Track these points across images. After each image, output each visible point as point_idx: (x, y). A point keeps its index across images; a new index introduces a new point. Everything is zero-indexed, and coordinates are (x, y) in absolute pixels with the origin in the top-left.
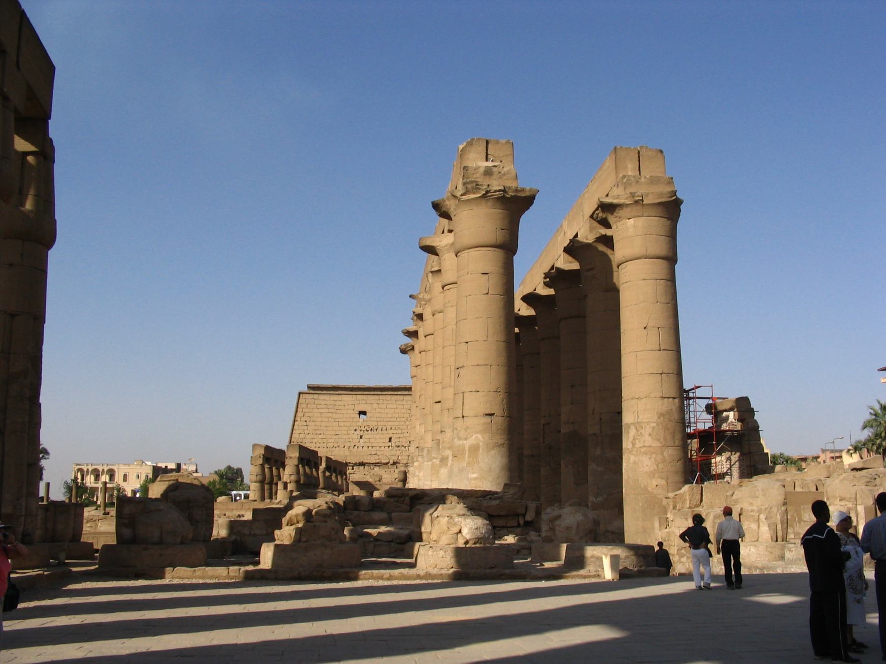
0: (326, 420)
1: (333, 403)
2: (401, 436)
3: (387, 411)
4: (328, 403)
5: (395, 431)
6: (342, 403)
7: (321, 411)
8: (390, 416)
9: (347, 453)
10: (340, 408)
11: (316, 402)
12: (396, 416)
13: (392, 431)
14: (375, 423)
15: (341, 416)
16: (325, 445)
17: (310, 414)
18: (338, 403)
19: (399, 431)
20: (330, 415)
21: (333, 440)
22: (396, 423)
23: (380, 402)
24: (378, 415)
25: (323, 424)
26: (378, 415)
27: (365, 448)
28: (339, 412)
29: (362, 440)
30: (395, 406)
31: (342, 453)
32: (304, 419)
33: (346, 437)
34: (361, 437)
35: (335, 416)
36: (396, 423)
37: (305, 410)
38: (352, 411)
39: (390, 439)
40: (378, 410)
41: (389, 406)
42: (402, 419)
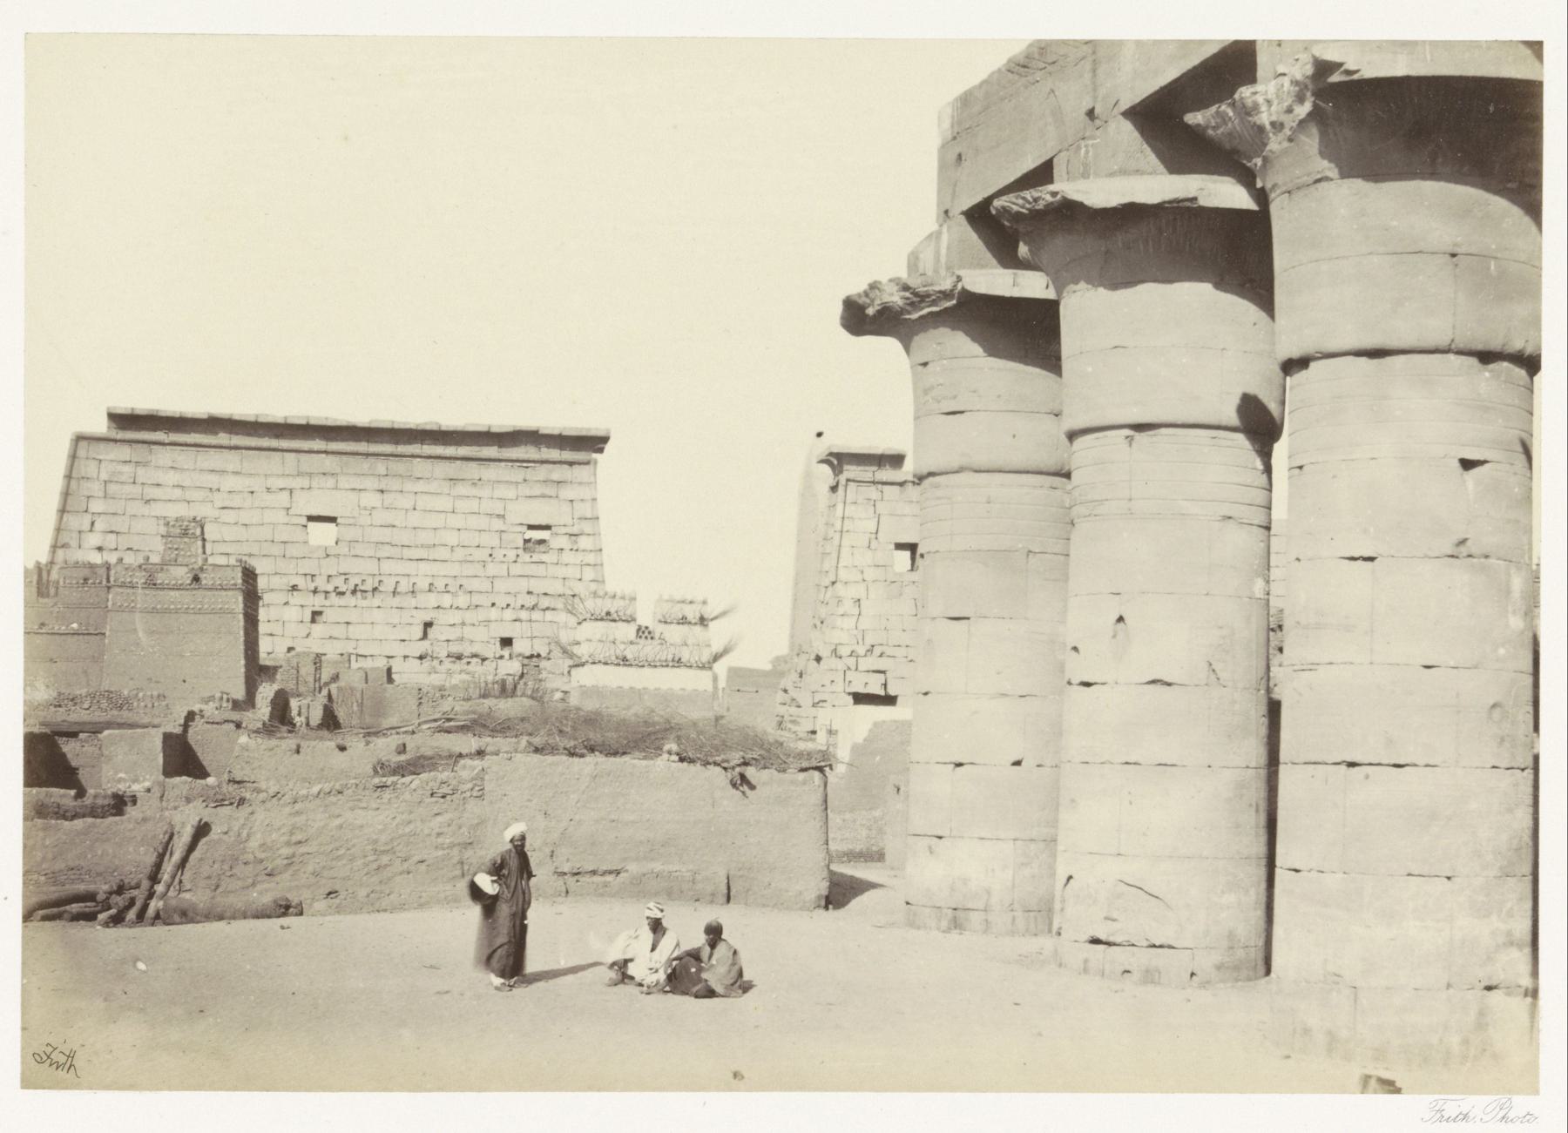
2: (470, 616)
3: (415, 519)
5: (447, 600)
8: (424, 537)
10: (236, 501)
13: (432, 600)
14: (371, 567)
17: (119, 524)
18: (230, 482)
19: (463, 600)
26: (385, 534)
28: (230, 516)
29: (318, 629)
34: (316, 615)
36: (454, 569)
38: (281, 517)
40: (381, 517)
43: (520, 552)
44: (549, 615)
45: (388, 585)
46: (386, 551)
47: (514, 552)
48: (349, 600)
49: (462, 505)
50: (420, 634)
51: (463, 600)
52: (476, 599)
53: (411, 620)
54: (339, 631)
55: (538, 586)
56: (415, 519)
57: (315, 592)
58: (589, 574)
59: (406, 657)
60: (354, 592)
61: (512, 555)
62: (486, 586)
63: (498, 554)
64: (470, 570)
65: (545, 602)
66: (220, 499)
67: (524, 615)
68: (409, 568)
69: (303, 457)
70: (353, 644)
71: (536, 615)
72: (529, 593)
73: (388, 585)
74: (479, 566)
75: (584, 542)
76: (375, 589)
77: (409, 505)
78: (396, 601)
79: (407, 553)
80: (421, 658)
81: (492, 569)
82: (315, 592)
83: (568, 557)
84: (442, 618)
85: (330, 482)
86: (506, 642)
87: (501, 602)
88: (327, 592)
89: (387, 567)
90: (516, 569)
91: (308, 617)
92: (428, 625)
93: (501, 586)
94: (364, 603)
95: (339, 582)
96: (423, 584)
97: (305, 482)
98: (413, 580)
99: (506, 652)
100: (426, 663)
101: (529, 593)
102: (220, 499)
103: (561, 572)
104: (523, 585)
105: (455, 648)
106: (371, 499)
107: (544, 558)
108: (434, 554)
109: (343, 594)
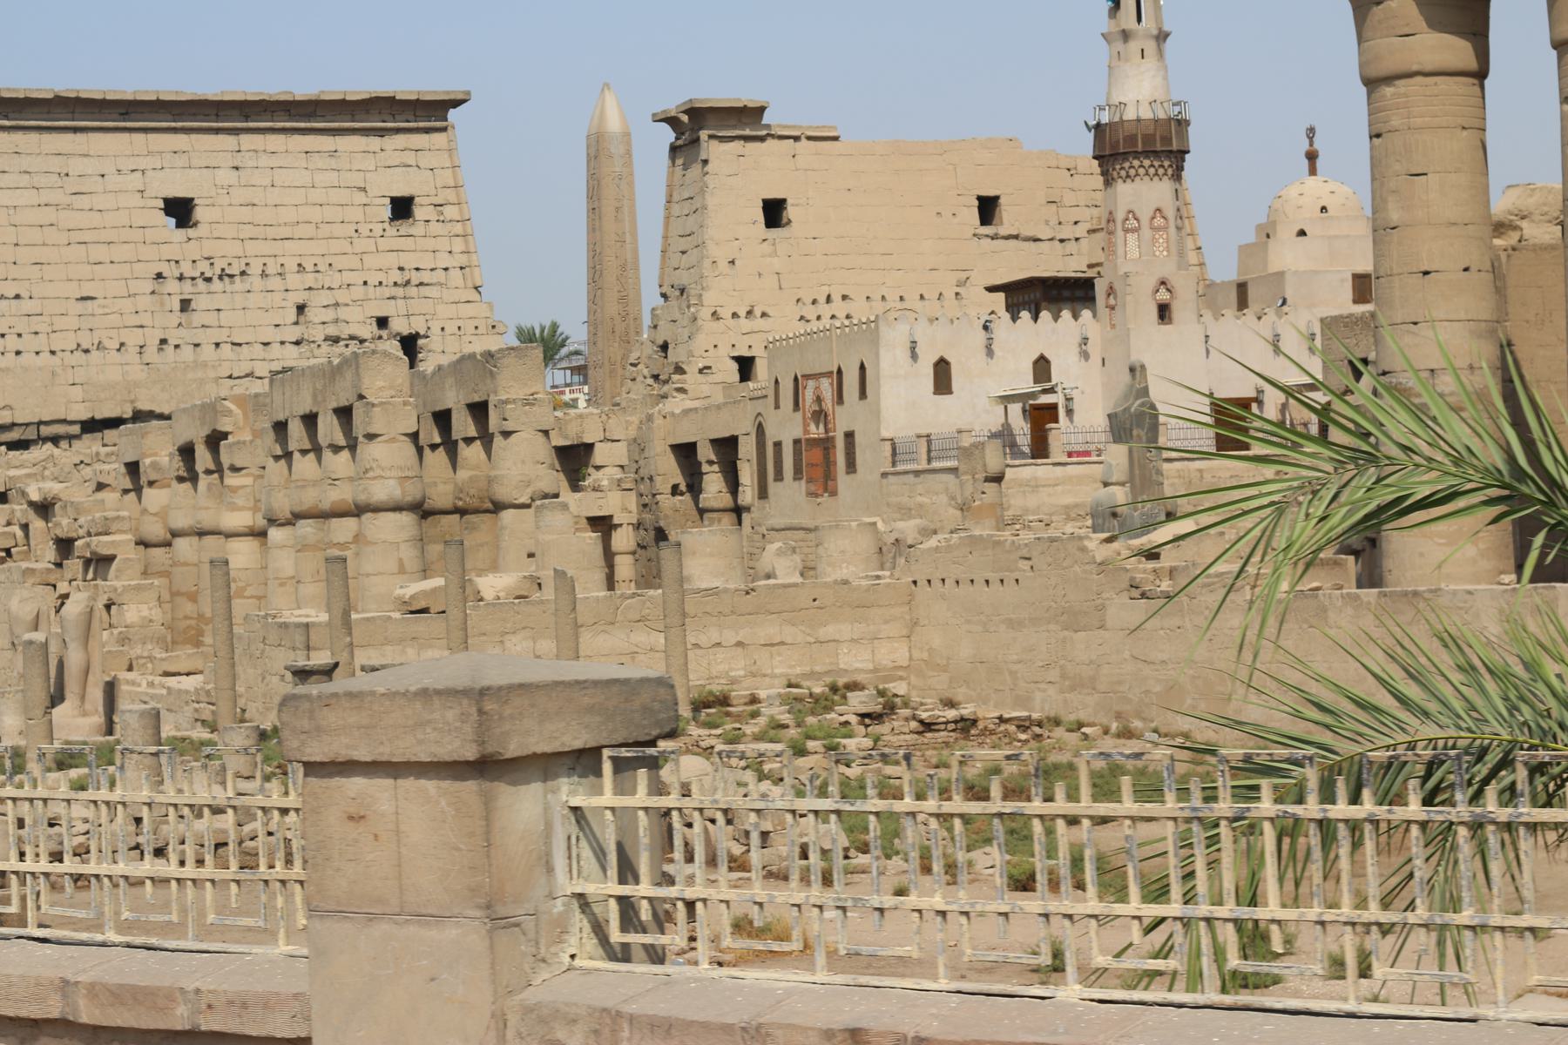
0: (35, 235)
3: (274, 196)
6: (90, 166)
8: (289, 215)
9: (137, 373)
12: (315, 214)
14: (236, 248)
16: (41, 342)
18: (76, 166)
20: (48, 215)
21: (73, 322)
22: (317, 247)
23: (247, 160)
25: (24, 254)
27: (208, 352)
28: (83, 202)
30: (303, 178)
31: (114, 374)
33: (127, 305)
34: (185, 305)
35: (67, 219)
36: (317, 247)
38: (136, 200)
39: (301, 309)
40: (240, 195)
41: (281, 177)
42: (338, 230)
43: (386, 225)
44: (424, 291)
45: (255, 269)
46: (248, 231)
48: (217, 285)
49: (320, 178)
50: (293, 318)
51: (335, 280)
52: (348, 277)
53: (284, 304)
54: (210, 319)
55: (409, 261)
56: (274, 196)
57: (181, 278)
58: (458, 245)
59: (282, 343)
60: (220, 278)
61: (378, 229)
62: (356, 264)
63: (364, 230)
64: (336, 246)
65: (416, 278)
67: (400, 292)
68: (277, 247)
69: (152, 136)
70: (225, 332)
71: (412, 291)
72: (401, 269)
74: (346, 243)
75: (451, 212)
76: (243, 273)
77: (268, 182)
79: (271, 232)
80: (297, 343)
81: (362, 244)
82: (181, 278)
83: (435, 228)
84: (318, 300)
85: (180, 161)
86: (382, 322)
87: (373, 281)
88: (193, 279)
89: (252, 248)
91: (177, 306)
92: (301, 309)
93: (370, 261)
94: (229, 288)
95: (203, 266)
96: (291, 265)
99: (384, 333)
100: (304, 348)
101: (401, 269)
102: (72, 185)
103: (430, 244)
104: (393, 260)
105: (332, 330)
106: (225, 176)
107: (412, 231)
109: (208, 280)
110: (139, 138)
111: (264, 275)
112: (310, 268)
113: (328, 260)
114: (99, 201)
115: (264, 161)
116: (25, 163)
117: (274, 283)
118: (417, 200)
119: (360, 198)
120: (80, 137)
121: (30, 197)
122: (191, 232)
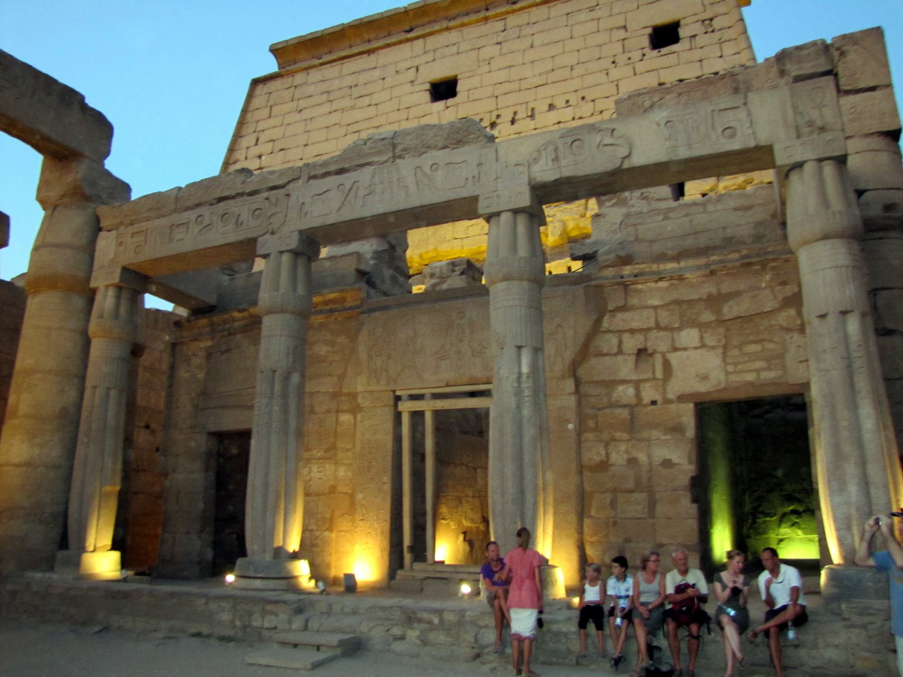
1: (350, 80)
3: (530, 55)
4: (336, 84)
6: (377, 74)
7: (306, 114)
10: (370, 88)
11: (298, 93)
12: (572, 59)
14: (490, 104)
15: (371, 111)
17: (275, 133)
18: (363, 78)
20: (336, 118)
24: (503, 75)
26: (503, 75)
28: (366, 101)
32: (255, 151)
35: (349, 117)
37: (261, 126)
38: (408, 88)
43: (647, 51)
47: (640, 53)
52: (600, 105)
61: (637, 55)
64: (590, 80)
66: (356, 92)
73: (507, 115)
77: (526, 43)
78: (517, 127)
79: (524, 85)
81: (615, 73)
85: (454, 49)
90: (640, 67)
96: (541, 107)
97: (429, 57)
98: (531, 106)
108: (552, 77)
110: (420, 42)
111: (513, 122)
112: (560, 102)
113: (580, 94)
114: (375, 99)
115: (527, 31)
116: (324, 87)
117: (524, 125)
118: (682, 23)
119: (622, 34)
120: (373, 57)
121: (327, 108)
122: (450, 101)
